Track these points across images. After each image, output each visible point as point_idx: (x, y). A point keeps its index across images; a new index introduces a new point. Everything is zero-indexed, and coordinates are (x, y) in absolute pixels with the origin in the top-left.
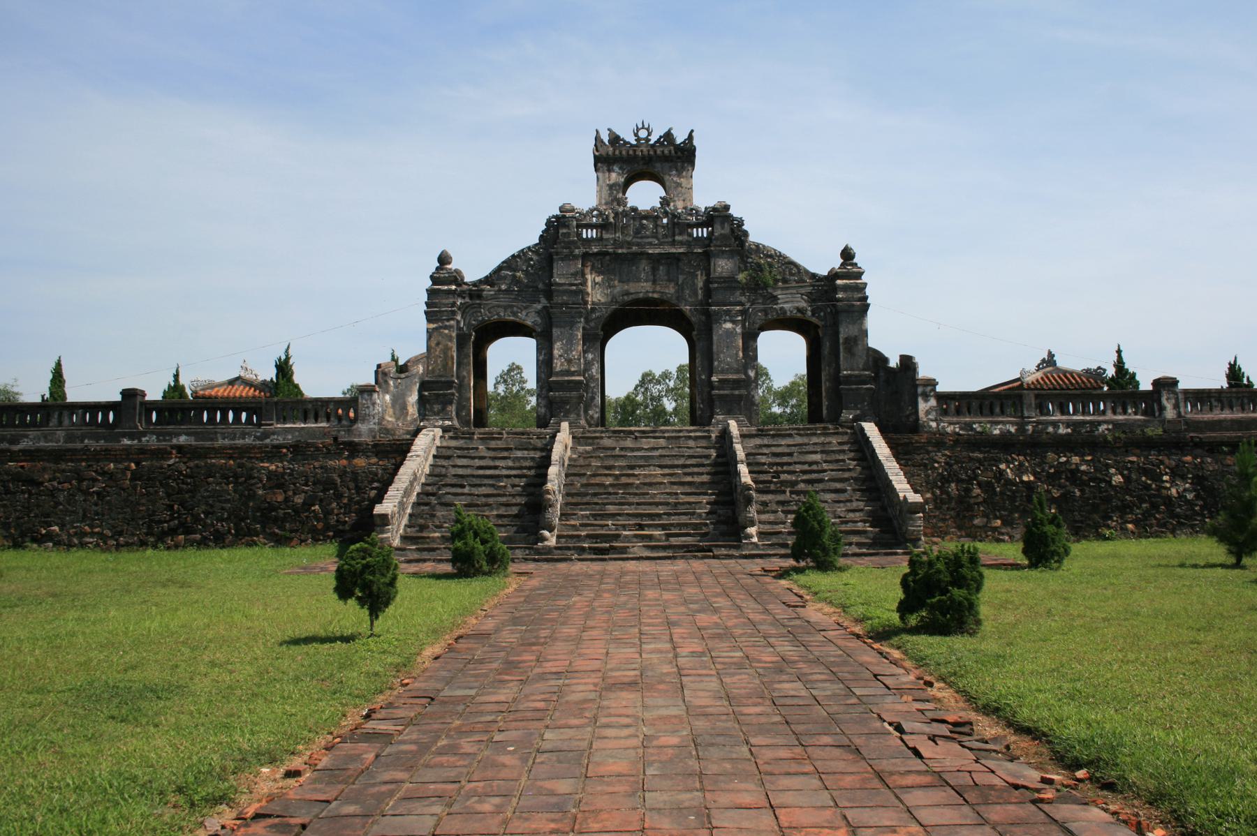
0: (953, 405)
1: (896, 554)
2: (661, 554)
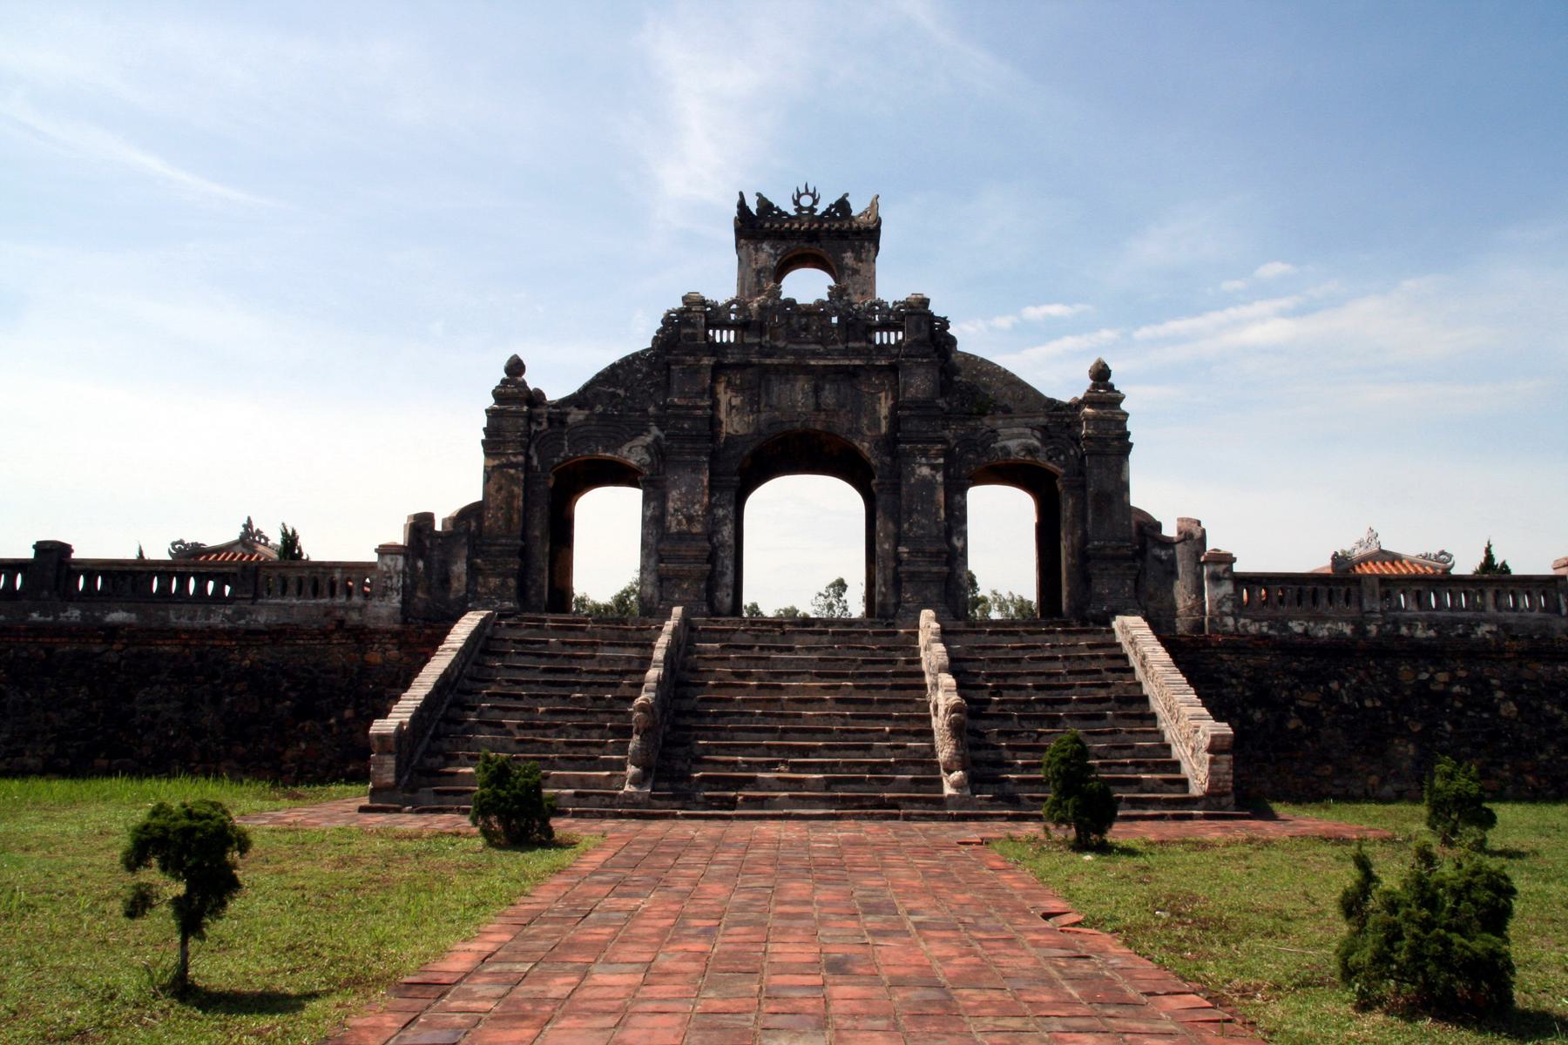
0: (1292, 590)
1: (1190, 817)
2: (1150, 812)
